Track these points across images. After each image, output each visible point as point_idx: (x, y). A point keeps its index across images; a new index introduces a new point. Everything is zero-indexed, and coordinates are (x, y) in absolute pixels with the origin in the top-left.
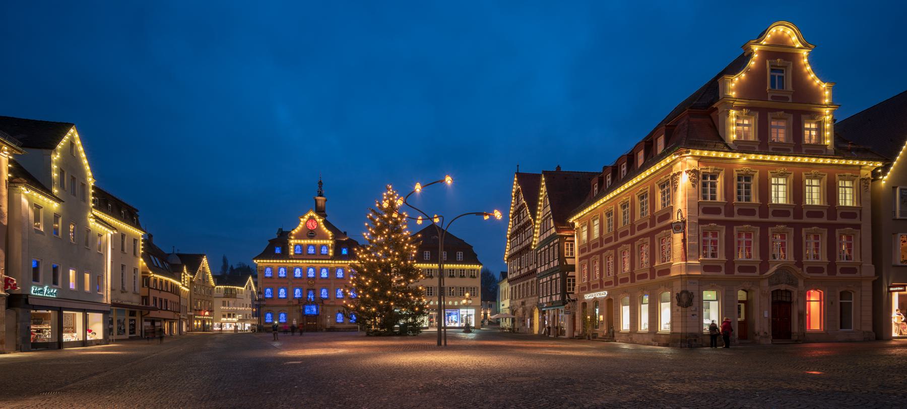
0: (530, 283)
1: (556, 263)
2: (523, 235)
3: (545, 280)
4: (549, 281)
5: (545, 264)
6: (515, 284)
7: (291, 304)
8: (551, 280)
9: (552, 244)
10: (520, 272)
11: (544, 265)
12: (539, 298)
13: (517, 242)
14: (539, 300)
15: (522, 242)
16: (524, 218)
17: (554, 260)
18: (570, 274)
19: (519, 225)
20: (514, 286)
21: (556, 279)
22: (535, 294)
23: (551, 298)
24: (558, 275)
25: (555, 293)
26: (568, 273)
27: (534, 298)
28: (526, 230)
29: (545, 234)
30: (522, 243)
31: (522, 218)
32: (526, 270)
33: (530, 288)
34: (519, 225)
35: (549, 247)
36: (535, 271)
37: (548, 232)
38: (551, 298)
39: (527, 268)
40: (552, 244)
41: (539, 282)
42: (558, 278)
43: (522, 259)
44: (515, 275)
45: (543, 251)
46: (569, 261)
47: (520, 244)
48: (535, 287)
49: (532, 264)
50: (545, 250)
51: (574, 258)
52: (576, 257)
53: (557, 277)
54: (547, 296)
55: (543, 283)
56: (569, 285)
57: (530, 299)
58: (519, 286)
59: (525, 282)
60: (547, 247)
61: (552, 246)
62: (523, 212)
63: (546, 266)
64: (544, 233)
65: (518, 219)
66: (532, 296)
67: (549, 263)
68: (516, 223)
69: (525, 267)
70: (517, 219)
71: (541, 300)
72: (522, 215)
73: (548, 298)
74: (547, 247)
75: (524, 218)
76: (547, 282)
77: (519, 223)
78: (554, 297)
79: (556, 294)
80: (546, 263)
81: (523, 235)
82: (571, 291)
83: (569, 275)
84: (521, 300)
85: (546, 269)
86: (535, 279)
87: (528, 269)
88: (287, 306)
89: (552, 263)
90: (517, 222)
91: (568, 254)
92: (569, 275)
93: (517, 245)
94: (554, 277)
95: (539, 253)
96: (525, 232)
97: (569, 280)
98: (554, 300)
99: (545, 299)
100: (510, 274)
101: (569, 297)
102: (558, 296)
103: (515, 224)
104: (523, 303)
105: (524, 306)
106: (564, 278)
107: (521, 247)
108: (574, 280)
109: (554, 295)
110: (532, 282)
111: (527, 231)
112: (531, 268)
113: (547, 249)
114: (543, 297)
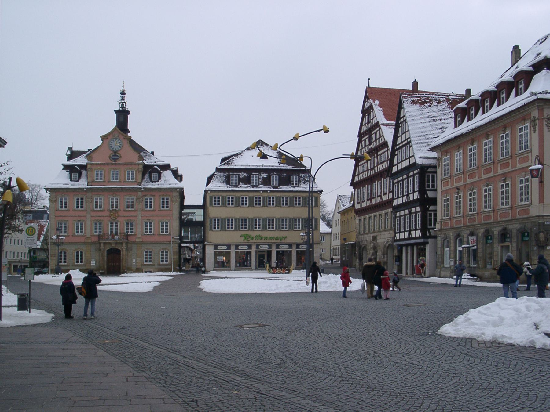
0: (383, 215)
1: (416, 196)
2: (376, 159)
3: (402, 213)
4: (407, 214)
5: (403, 196)
6: (364, 215)
7: (90, 241)
8: (410, 213)
9: (411, 174)
10: (371, 202)
11: (403, 197)
12: (396, 233)
13: (367, 166)
14: (395, 236)
15: (374, 167)
16: (376, 139)
17: (414, 192)
18: (432, 208)
19: (370, 147)
20: (362, 217)
21: (416, 213)
22: (389, 228)
23: (410, 234)
24: (418, 209)
25: (403, 230)
26: (429, 207)
27: (388, 232)
28: (379, 153)
29: (403, 163)
30: (373, 169)
31: (374, 139)
32: (379, 200)
33: (383, 221)
34: (370, 147)
35: (408, 177)
36: (390, 201)
37: (407, 161)
38: (410, 234)
39: (380, 197)
40: (411, 174)
41: (396, 215)
42: (419, 212)
43: (374, 188)
44: (364, 205)
45: (400, 181)
46: (430, 194)
47: (372, 169)
48: (389, 220)
49: (386, 194)
50: (403, 180)
51: (436, 190)
52: (438, 190)
53: (417, 211)
54: (405, 231)
55: (400, 217)
56: (430, 220)
57: (382, 233)
58: (370, 218)
59: (378, 213)
60: (405, 176)
61: (411, 176)
62: (376, 133)
63: (405, 198)
64: (402, 161)
65: (369, 140)
66: (385, 230)
67: (408, 195)
68: (367, 144)
69: (378, 196)
70: (367, 140)
71: (397, 235)
72: (373, 136)
73: (407, 233)
74: (405, 176)
75: (376, 139)
76: (405, 215)
77: (370, 144)
78: (413, 233)
79: (416, 230)
80: (405, 194)
81: (376, 159)
82: (433, 226)
83: (430, 209)
84: (372, 235)
85: (404, 201)
86: (390, 210)
87: (381, 198)
88: (85, 243)
89: (411, 196)
90: (367, 143)
91: (428, 186)
92: (430, 209)
93: (368, 170)
94: (413, 210)
95: (396, 183)
96: (377, 156)
97: (430, 215)
98: (413, 235)
99: (402, 234)
100: (358, 203)
101: (429, 233)
102: (418, 232)
103: (365, 146)
104: (375, 238)
105: (375, 242)
106: (424, 212)
107: (372, 173)
108: (435, 215)
109: (413, 230)
110: (386, 214)
111: (380, 155)
112: (385, 198)
113: (405, 179)
114: (400, 232)
